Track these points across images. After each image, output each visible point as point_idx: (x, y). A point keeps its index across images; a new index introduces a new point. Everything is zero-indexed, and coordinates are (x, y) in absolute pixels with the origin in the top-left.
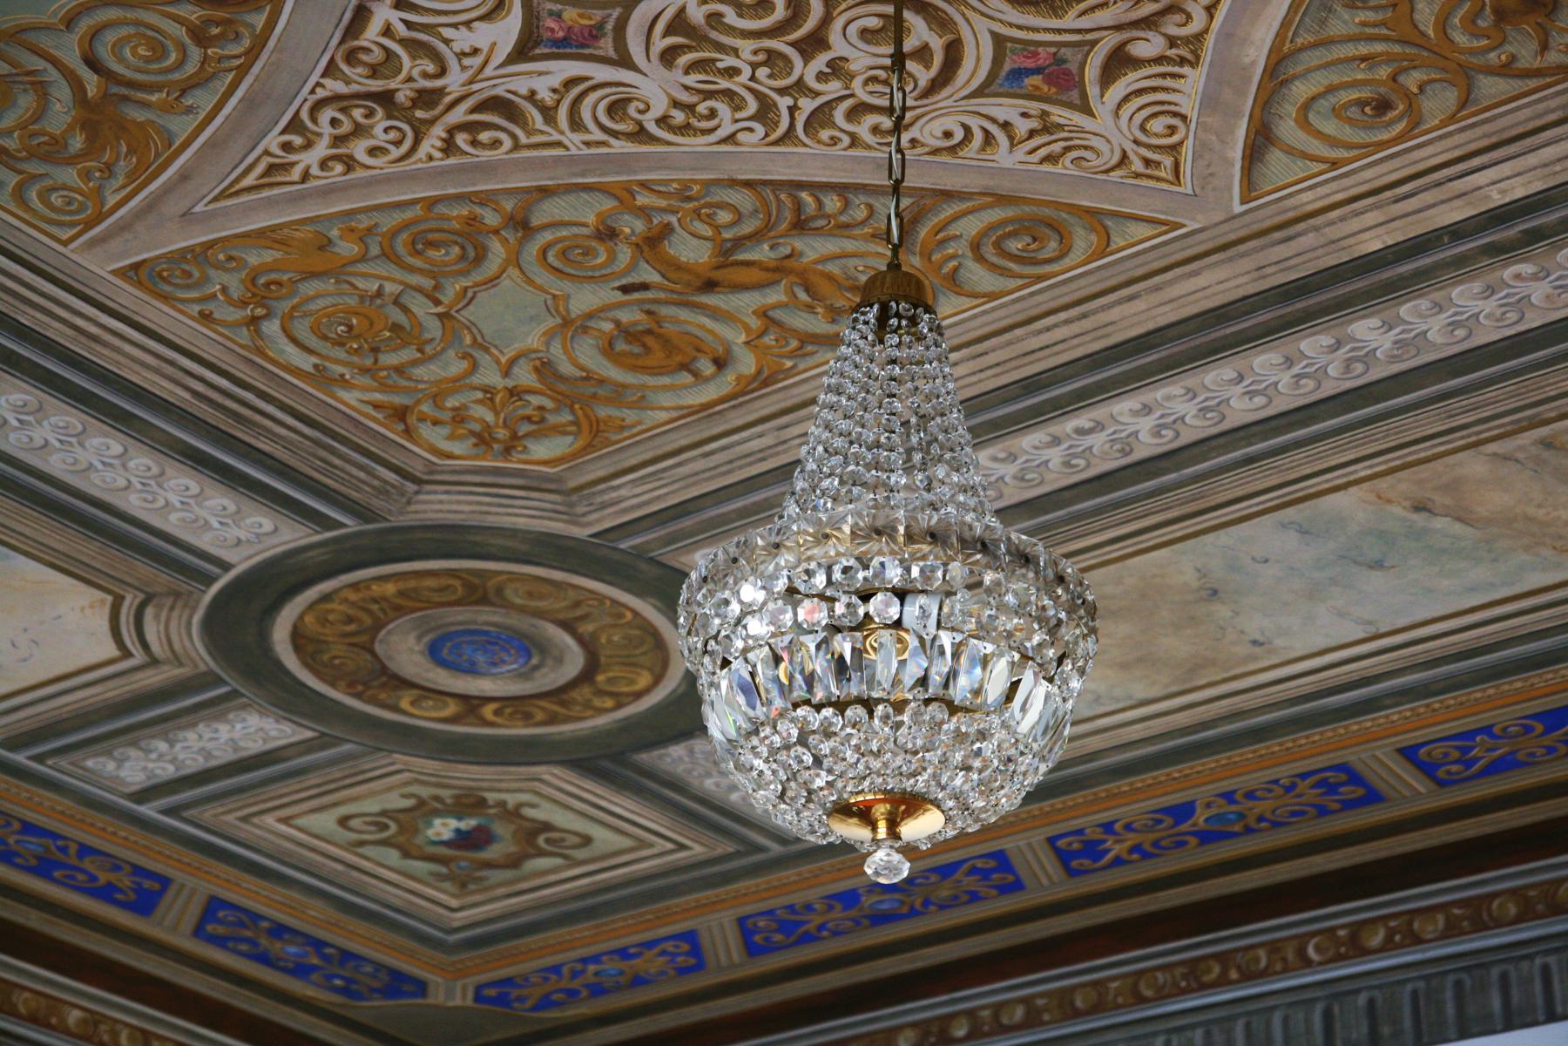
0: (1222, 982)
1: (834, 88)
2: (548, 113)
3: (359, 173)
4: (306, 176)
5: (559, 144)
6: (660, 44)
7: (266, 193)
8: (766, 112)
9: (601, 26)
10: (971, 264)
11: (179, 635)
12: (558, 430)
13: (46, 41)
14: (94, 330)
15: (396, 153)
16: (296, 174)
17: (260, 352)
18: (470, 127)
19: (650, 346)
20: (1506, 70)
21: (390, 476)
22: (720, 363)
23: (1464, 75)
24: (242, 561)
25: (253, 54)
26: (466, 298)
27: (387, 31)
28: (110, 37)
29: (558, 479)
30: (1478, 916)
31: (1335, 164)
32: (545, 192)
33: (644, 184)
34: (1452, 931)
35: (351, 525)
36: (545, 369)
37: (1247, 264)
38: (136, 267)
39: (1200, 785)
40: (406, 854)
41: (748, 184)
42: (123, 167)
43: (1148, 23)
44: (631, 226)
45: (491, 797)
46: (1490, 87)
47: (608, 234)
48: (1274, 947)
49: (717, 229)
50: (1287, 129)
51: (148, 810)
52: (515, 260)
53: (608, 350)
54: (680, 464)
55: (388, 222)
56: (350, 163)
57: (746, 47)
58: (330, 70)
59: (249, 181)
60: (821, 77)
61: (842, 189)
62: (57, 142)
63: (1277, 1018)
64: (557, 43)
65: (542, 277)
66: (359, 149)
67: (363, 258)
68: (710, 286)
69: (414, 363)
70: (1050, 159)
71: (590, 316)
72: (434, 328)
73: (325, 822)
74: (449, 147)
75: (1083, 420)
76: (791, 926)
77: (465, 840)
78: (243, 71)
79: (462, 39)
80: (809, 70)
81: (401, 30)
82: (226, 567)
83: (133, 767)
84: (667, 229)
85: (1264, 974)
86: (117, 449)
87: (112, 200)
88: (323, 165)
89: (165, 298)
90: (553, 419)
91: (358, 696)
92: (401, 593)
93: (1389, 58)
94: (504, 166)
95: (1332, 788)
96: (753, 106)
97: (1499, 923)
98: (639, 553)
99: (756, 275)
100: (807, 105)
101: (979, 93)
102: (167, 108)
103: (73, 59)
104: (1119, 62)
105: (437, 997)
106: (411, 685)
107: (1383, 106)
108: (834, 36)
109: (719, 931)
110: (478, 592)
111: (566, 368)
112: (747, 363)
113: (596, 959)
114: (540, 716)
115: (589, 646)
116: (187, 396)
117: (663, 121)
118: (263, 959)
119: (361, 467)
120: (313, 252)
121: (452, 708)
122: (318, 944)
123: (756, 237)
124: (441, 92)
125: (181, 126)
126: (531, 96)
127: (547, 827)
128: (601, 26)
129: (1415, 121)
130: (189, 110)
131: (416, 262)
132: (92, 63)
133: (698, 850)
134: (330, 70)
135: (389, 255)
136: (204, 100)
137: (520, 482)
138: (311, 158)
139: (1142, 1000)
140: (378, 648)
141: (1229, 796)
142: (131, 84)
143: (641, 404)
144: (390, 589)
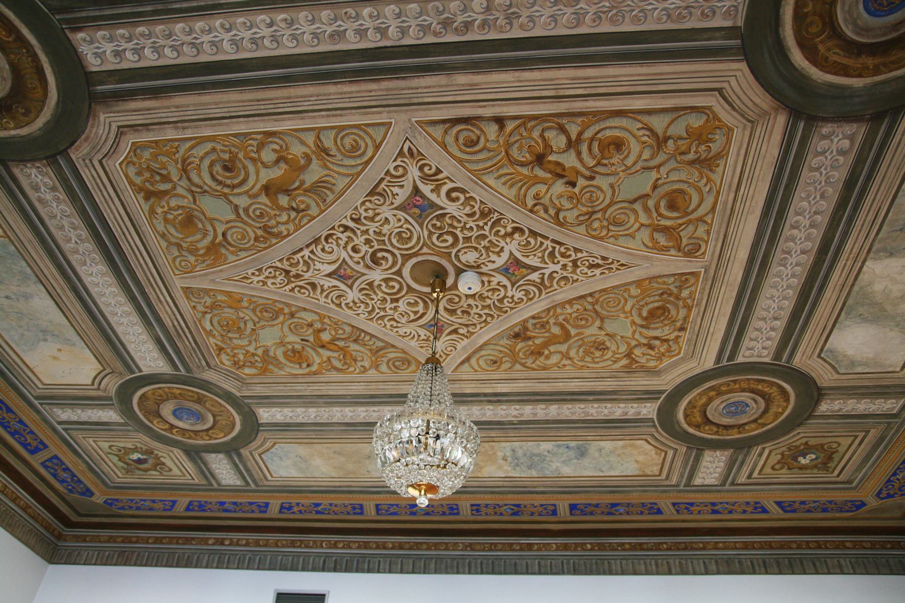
0: (300, 547)
1: (391, 312)
2: (323, 291)
3: (265, 287)
4: (251, 283)
6: (363, 286)
9: (352, 277)
10: (385, 364)
11: (112, 385)
12: (256, 368)
13: (217, 224)
14: (162, 299)
15: (278, 286)
16: (250, 281)
17: (200, 321)
18: (301, 287)
19: (297, 356)
20: (523, 365)
21: (204, 363)
22: (308, 366)
23: (515, 362)
24: (146, 371)
25: (265, 248)
26: (263, 327)
27: (302, 257)
28: (234, 230)
29: (245, 379)
30: (366, 545)
31: (476, 371)
32: (305, 309)
33: (329, 317)
34: (359, 547)
35: (183, 371)
36: (266, 352)
38: (188, 288)
39: (325, 501)
40: (120, 460)
41: (353, 326)
43: (467, 326)
44: (318, 325)
45: (156, 452)
46: (518, 367)
47: (310, 325)
48: (315, 542)
49: (336, 334)
50: (473, 361)
51: (59, 427)
52: (282, 323)
53: (285, 354)
55: (261, 301)
56: (265, 283)
57: (380, 295)
58: (281, 260)
60: (391, 309)
61: (372, 336)
62: (197, 250)
63: (312, 559)
64: (340, 276)
65: (286, 329)
66: (270, 282)
67: (247, 308)
68: (323, 347)
69: (236, 338)
70: (422, 347)
71: (288, 343)
72: (249, 331)
73: (105, 445)
74: (292, 290)
75: (376, 409)
76: (202, 507)
77: (139, 461)
78: (260, 251)
79: (318, 266)
80: (388, 305)
81: (306, 258)
82: (140, 371)
83: (66, 414)
84: (325, 329)
85: (311, 547)
86: (140, 331)
87: (197, 269)
88: (258, 282)
89: (188, 298)
90: (257, 364)
91: (145, 416)
92: (180, 394)
93: (506, 353)
94: (301, 299)
95: (354, 508)
96: (370, 309)
97: (371, 548)
98: (248, 405)
99: (336, 348)
100: (382, 313)
101: (420, 326)
102: (233, 253)
103: (220, 231)
104: (455, 331)
105: (93, 499)
106: (160, 417)
107: (495, 362)
108: (401, 302)
109: (183, 502)
110: (200, 400)
111: (271, 354)
112: (314, 368)
113: (145, 501)
114: (187, 436)
115: (215, 422)
116: (171, 324)
117: (347, 304)
118: (55, 476)
119: (199, 359)
120: (235, 301)
121: (167, 426)
122: (74, 475)
123: (343, 339)
124: (302, 276)
125: (231, 258)
126: (322, 286)
127: (164, 464)
128: (352, 277)
129: (499, 367)
130: (237, 255)
131: (259, 314)
133: (197, 481)
134: (281, 260)
135: (254, 310)
136: (243, 254)
138: (256, 279)
139: (277, 546)
140: (161, 406)
141: (331, 505)
142: (229, 244)
143: (281, 369)
144: (178, 391)
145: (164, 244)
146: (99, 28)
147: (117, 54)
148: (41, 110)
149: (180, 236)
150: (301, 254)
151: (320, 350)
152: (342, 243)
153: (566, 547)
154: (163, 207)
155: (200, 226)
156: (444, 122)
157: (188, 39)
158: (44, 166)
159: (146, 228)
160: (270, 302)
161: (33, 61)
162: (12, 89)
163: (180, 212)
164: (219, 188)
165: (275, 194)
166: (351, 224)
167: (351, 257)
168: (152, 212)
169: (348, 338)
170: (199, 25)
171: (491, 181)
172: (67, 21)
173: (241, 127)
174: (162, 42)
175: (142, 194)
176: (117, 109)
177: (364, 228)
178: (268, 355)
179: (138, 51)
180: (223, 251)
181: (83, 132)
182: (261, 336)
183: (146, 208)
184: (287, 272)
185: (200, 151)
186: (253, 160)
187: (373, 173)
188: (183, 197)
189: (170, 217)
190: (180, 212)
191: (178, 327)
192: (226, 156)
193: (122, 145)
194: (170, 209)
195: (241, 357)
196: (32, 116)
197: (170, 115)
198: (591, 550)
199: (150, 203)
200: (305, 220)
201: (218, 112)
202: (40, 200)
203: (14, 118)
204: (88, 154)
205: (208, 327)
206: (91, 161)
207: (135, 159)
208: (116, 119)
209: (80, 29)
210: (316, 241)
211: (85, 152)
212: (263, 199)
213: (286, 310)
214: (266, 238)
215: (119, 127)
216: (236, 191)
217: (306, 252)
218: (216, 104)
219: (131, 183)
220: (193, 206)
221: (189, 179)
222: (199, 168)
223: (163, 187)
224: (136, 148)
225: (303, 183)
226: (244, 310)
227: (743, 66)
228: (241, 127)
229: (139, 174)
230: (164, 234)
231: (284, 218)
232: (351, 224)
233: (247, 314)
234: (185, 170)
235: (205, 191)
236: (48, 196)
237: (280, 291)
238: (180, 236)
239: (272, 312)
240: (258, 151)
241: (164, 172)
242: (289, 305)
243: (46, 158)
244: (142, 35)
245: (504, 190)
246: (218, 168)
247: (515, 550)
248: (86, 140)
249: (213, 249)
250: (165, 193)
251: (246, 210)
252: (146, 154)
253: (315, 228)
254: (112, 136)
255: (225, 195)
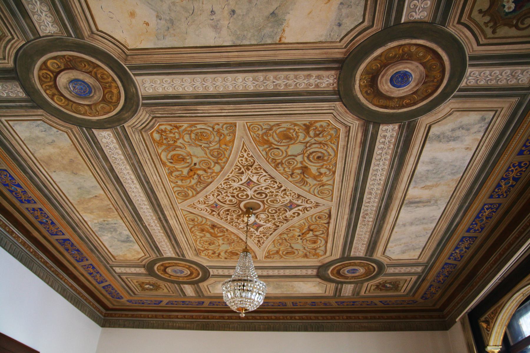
2: (238, 176)
3: (238, 157)
4: (241, 152)
5: (231, 173)
7: (241, 147)
8: (224, 189)
15: (240, 162)
18: (240, 169)
37: (167, 205)
38: (236, 126)
41: (211, 182)
42: (257, 139)
54: (143, 145)
55: (227, 154)
59: (245, 147)
67: (220, 146)
78: (266, 159)
87: (252, 133)
89: (226, 123)
100: (223, 192)
112: (168, 164)
132: (278, 149)
135: (219, 149)
136: (264, 153)
137: (148, 127)
145: (272, 124)
146: (397, 134)
147: (385, 137)
148: (367, 100)
149: (277, 132)
150: (263, 172)
151: (188, 169)
152: (271, 185)
153: (24, 244)
154: (298, 130)
155: (284, 141)
156: (330, 213)
157: (383, 158)
158: (334, 88)
159: (284, 119)
160: (227, 156)
161: (392, 107)
162: (381, 93)
163: (295, 136)
164: (308, 152)
165: (303, 170)
166: (282, 189)
167: (262, 187)
168: (296, 125)
169: (201, 180)
170: (387, 163)
171: (302, 221)
172: (404, 125)
173: (340, 166)
174: (384, 151)
175: (308, 124)
176: (360, 128)
177: (280, 192)
178: (176, 147)
179: (383, 143)
180: (266, 146)
181: (351, 112)
182: (195, 148)
183: (298, 123)
184: (251, 166)
185: (330, 150)
186: (323, 166)
187: (309, 196)
188: (304, 139)
189: (292, 131)
190: (295, 136)
191: (196, 112)
192: (326, 158)
193: (340, 125)
194: (297, 132)
195: (172, 135)
196: (365, 95)
197: (352, 145)
198: (31, 253)
199: (302, 125)
200: (285, 176)
201: (348, 160)
202: (309, 76)
203: (366, 86)
204: (338, 110)
205: (199, 126)
206: (333, 109)
207: (330, 127)
208: (354, 127)
209: (399, 128)
210: (272, 178)
211: (339, 109)
212: (299, 165)
213: (220, 161)
214: (275, 162)
215: (350, 127)
216: (306, 158)
217: (265, 174)
218: (353, 160)
219: (316, 122)
220: (298, 141)
221: (315, 144)
222: (320, 148)
223: (312, 133)
224: (337, 130)
225: (308, 178)
226: (218, 145)
227: (338, 257)
228: (340, 166)
229: (321, 126)
230: (279, 126)
231: (287, 169)
232: (282, 189)
233: (214, 146)
234: (320, 143)
235: (307, 148)
236: (312, 81)
237: (237, 161)
238: (277, 132)
239: (219, 157)
240: (326, 168)
241: (321, 136)
242: (226, 163)
243: (339, 90)
244: (389, 146)
245: (299, 223)
246: (320, 154)
247: (5, 230)
248: (346, 111)
249: (267, 142)
250: (308, 133)
251: (293, 159)
252: (332, 132)
253: (280, 178)
254: (346, 123)
255: (304, 154)
